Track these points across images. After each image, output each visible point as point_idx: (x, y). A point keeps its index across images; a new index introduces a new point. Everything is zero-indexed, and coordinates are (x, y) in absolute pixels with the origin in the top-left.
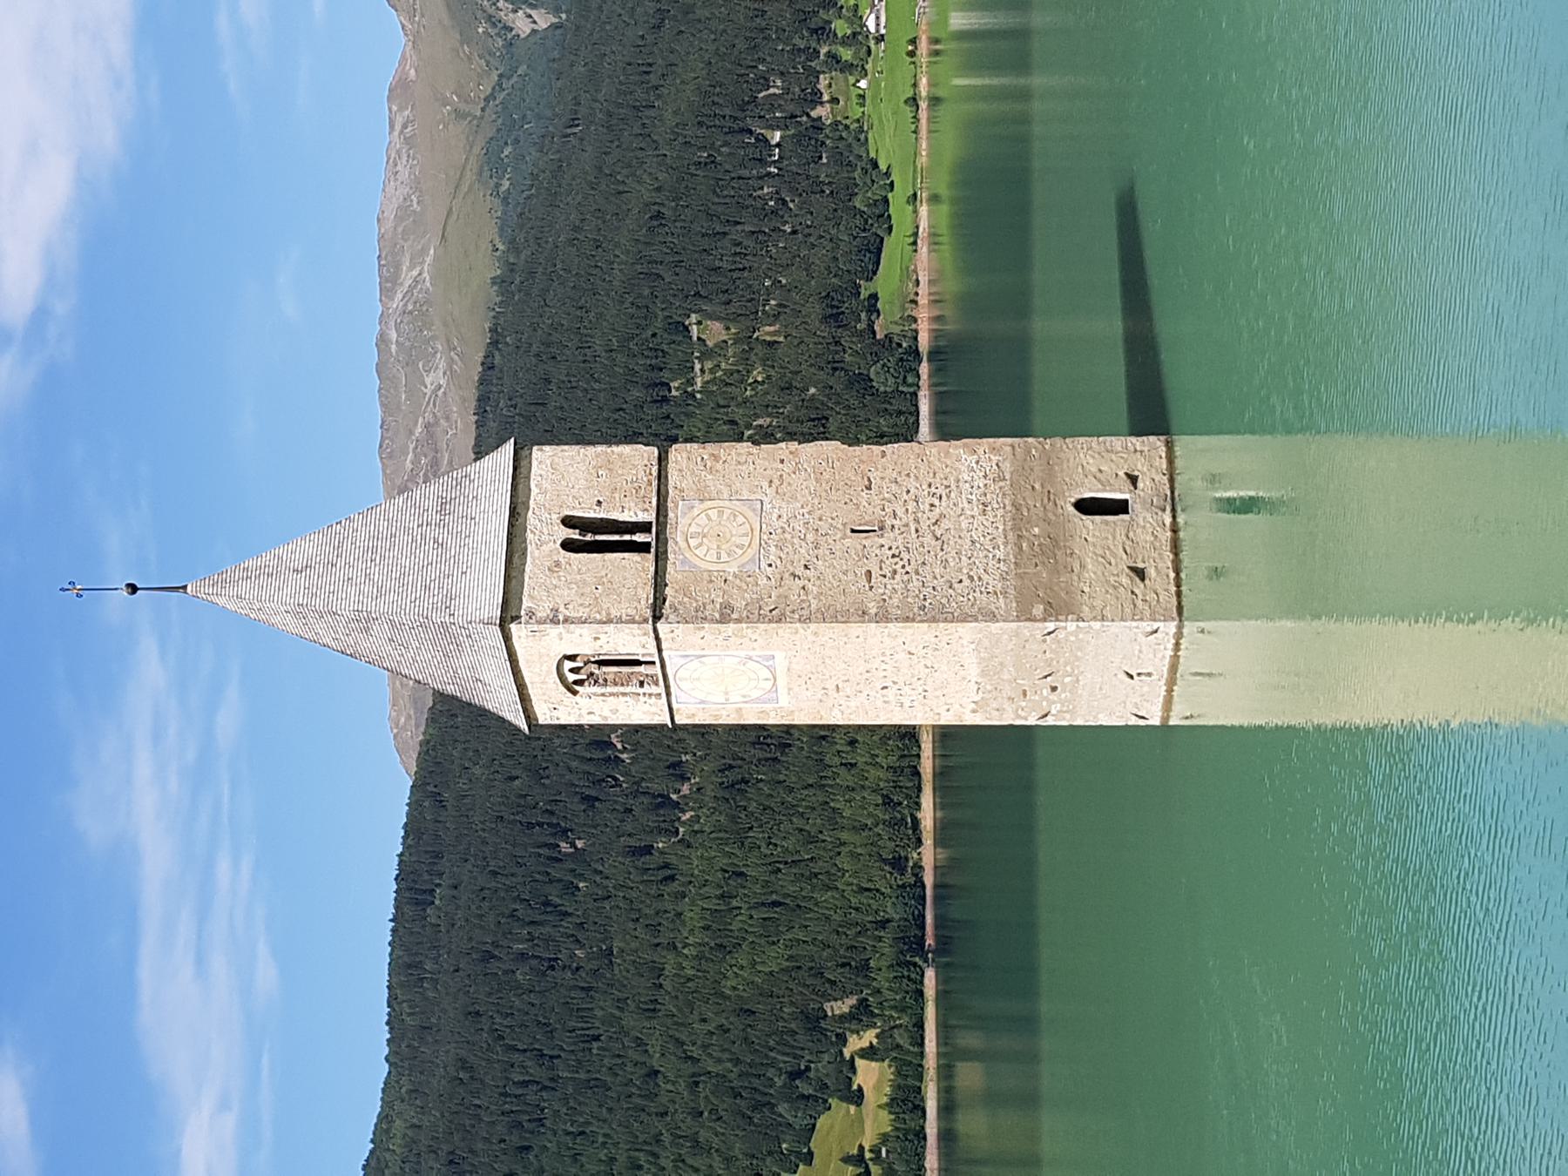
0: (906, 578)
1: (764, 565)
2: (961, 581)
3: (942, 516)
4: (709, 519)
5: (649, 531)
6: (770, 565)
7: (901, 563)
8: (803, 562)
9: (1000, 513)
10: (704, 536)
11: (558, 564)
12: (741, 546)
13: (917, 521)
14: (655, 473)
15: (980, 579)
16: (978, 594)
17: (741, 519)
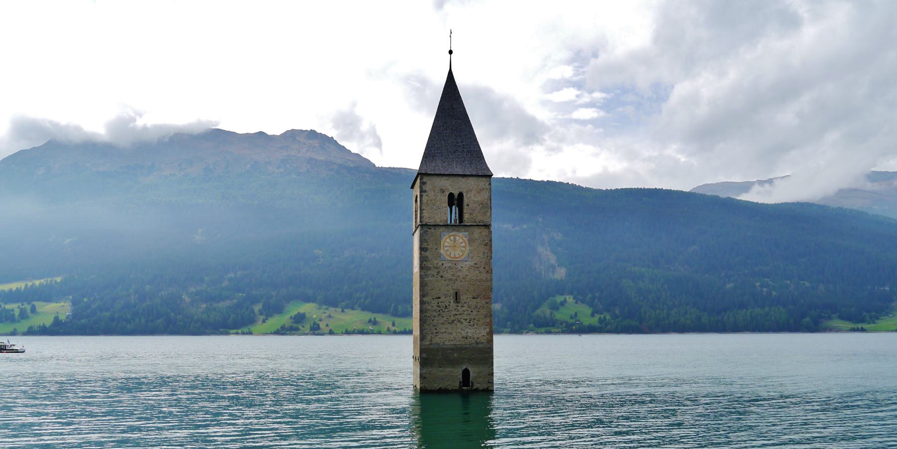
0: (438, 310)
1: (443, 262)
2: (436, 329)
3: (462, 323)
4: (461, 243)
5: (459, 223)
6: (443, 264)
7: (443, 309)
8: (444, 276)
9: (464, 344)
10: (454, 242)
11: (443, 192)
12: (450, 254)
13: (460, 314)
14: (479, 224)
15: (437, 336)
16: (431, 335)
17: (461, 254)
